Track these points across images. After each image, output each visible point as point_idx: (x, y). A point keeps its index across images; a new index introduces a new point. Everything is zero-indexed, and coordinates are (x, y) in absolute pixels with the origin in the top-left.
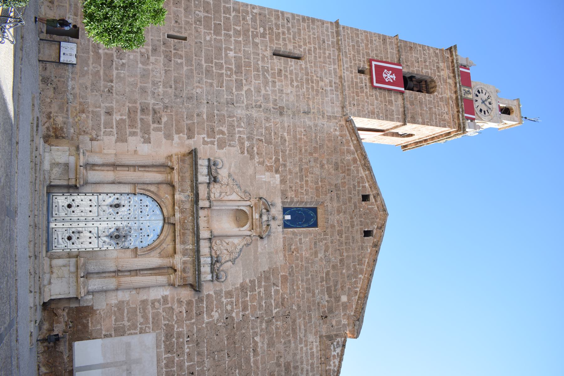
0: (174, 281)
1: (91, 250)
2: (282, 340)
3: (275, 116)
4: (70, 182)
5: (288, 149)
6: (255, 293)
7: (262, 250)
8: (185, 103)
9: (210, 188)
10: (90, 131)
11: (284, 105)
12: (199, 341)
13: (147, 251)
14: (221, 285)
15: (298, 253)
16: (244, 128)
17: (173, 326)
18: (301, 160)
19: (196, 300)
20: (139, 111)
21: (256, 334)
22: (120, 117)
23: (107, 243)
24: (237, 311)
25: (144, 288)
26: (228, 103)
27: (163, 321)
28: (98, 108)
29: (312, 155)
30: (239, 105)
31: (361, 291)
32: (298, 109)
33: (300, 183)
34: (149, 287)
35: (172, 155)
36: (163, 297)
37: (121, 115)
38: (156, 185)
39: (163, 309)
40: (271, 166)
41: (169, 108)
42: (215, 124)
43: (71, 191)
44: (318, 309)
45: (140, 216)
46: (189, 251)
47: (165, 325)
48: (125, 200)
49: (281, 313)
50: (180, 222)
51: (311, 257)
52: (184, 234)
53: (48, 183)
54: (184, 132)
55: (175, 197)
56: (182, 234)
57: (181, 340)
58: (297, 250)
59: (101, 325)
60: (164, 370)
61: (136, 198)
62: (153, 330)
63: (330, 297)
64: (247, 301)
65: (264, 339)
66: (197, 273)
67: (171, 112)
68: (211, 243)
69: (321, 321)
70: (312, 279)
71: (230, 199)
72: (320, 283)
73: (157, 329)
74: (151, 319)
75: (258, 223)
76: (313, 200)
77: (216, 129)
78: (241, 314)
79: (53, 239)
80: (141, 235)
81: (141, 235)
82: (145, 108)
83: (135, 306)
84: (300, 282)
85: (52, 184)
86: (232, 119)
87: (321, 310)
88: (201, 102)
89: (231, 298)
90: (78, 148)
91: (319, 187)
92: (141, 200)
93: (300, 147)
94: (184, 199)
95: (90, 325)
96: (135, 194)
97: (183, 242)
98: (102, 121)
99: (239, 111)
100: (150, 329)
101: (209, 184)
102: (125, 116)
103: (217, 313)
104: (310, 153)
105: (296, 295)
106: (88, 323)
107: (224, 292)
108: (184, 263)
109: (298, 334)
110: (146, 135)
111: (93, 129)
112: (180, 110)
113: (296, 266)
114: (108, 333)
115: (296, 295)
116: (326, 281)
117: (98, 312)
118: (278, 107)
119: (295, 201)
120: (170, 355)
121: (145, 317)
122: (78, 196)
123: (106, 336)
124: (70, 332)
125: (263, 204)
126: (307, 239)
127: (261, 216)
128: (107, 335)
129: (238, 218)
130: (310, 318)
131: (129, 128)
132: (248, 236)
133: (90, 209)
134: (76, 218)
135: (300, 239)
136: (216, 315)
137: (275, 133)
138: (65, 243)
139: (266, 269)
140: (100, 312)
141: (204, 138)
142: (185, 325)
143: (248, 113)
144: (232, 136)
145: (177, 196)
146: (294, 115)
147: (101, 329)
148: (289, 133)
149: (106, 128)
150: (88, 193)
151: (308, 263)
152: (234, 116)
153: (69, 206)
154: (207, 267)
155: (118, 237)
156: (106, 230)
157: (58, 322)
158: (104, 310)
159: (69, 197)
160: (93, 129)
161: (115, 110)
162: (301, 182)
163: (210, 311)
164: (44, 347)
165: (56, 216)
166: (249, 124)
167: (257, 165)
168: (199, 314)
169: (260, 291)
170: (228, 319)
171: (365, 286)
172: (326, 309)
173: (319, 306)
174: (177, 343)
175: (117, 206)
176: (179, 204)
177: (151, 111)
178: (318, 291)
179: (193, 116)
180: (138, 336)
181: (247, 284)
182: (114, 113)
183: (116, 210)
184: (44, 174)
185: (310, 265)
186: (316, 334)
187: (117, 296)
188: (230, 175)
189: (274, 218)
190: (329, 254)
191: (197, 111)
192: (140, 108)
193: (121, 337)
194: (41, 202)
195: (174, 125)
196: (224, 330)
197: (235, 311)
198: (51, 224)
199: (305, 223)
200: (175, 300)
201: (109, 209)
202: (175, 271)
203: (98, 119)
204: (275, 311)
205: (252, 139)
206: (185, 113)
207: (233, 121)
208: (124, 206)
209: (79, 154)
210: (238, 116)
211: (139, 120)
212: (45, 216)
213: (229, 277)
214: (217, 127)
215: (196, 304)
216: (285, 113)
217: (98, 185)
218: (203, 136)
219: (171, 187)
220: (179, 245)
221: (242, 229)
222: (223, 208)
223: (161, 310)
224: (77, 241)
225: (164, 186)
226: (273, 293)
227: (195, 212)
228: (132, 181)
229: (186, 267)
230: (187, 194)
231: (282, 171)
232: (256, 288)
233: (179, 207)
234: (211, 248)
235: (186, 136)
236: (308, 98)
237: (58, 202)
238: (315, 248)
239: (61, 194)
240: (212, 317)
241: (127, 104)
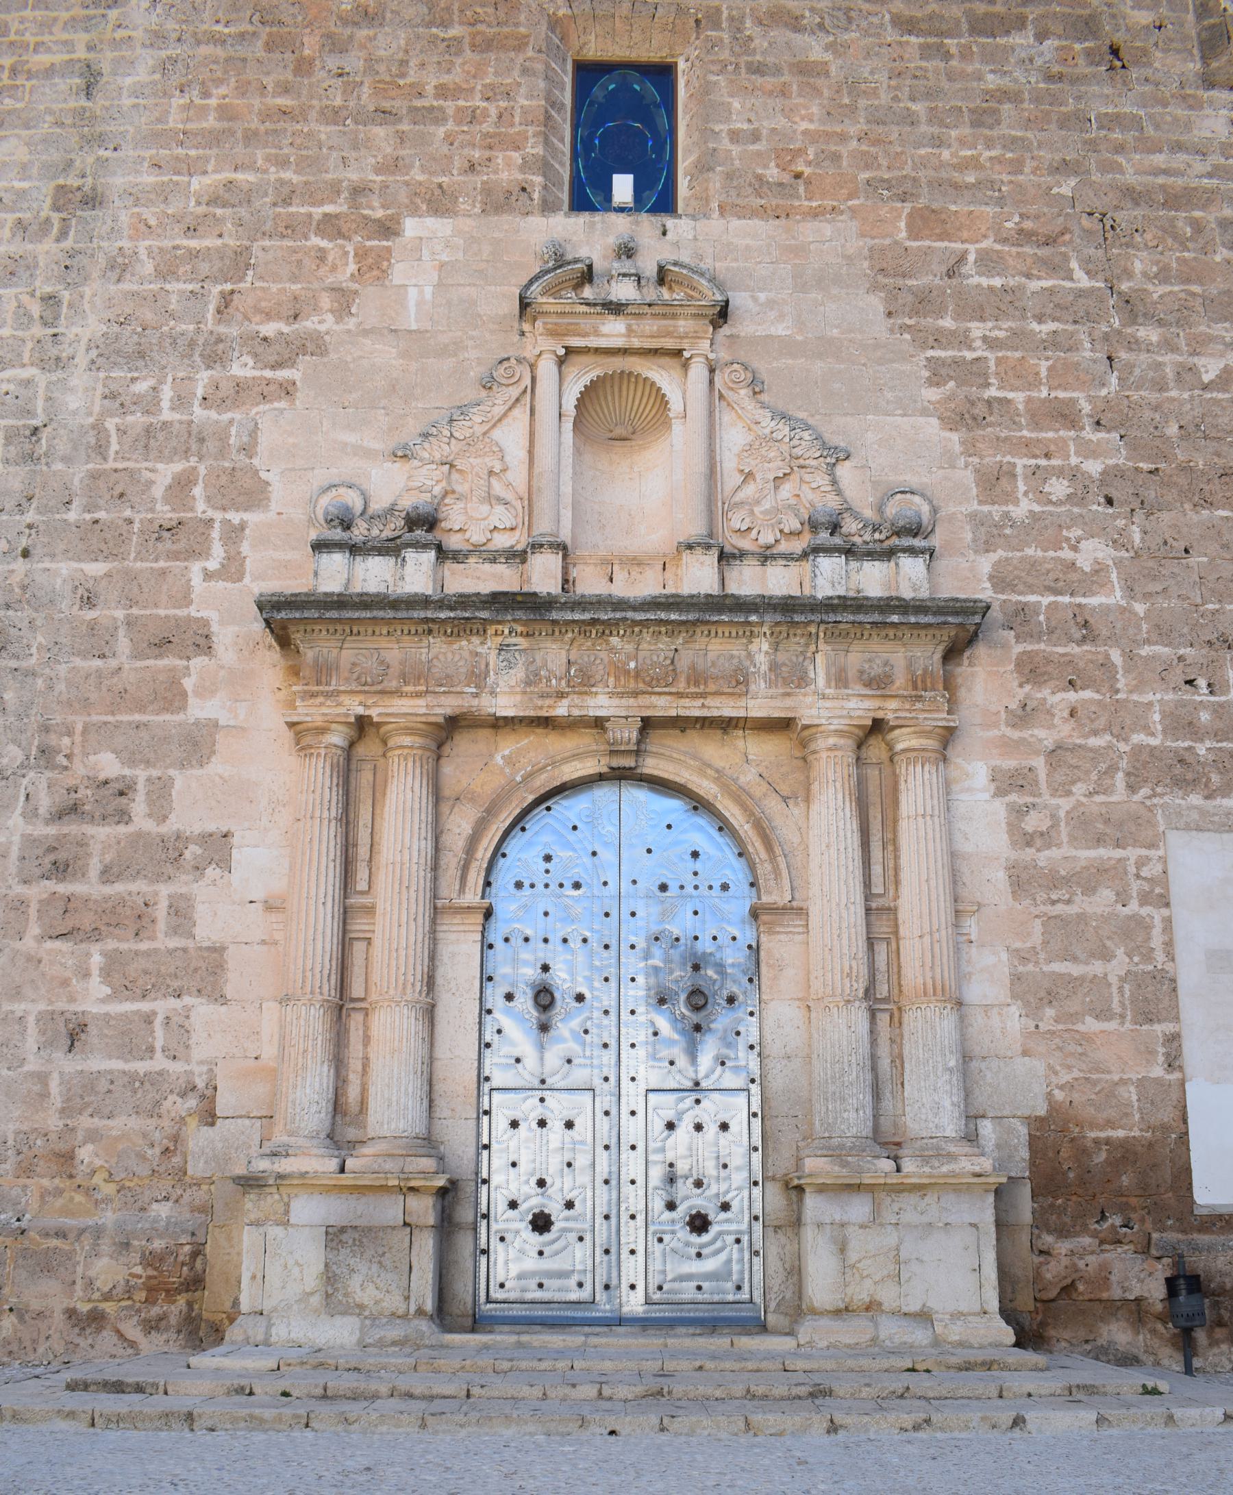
0: (923, 733)
1: (757, 1123)
2: (1218, 258)
3: (106, 228)
4: (422, 1222)
5: (273, 174)
6: (992, 364)
7: (781, 317)
8: (24, 664)
9: (465, 547)
10: (166, 1123)
11: (48, 188)
12: (1213, 637)
13: (773, 858)
14: (951, 518)
15: (801, 152)
16: (161, 382)
17: (1138, 749)
18: (333, 116)
19: (1017, 637)
20: (63, 888)
21: (1186, 374)
22: (96, 979)
23: (725, 1051)
24: (1077, 453)
25: (955, 878)
26: (30, 457)
27: (1114, 799)
28: (46, 1085)
29: (311, 62)
30: (40, 404)
32: (69, 121)
33: (450, 125)
34: (953, 855)
35: (291, 725)
36: (1000, 793)
37: (87, 975)
38: (445, 808)
39: (1054, 793)
40: (361, 255)
41: (53, 739)
42: (137, 518)
43: (465, 1214)
44: (1076, 80)
45: (598, 890)
46: (781, 657)
47: (1132, 788)
48: (515, 962)
49: (1092, 251)
50: (635, 694)
51: (826, 93)
52: (696, 677)
53: (424, 1325)
54: (172, 669)
55: (510, 713)
56: (697, 684)
57: (1205, 716)
58: (787, 156)
59: (1123, 1082)
61: (507, 905)
62: (1152, 846)
63: (1020, 23)
64: (1029, 400)
65: (1211, 339)
66: (895, 618)
67: (70, 733)
68: (741, 555)
69: (1134, 73)
70: (929, 95)
71: (523, 454)
72: (954, 63)
73: (1152, 824)
74: (1102, 852)
75: (650, 325)
76: (539, 67)
77: (165, 513)
78: (1089, 434)
79: (700, 1297)
80: (689, 889)
81: (689, 889)
82: (52, 857)
83: (1038, 922)
84: (946, 154)
85: (429, 1306)
86: (114, 439)
87: (1083, 67)
88: (24, 588)
89: (1014, 476)
90: (250, 1183)
91: (473, 36)
92: (519, 885)
93: (265, 116)
94: (519, 673)
95: (1121, 1133)
96: (488, 913)
97: (740, 682)
98: (117, 1065)
99: (74, 402)
100: (1148, 859)
101: (442, 553)
102: (88, 955)
103: (1084, 545)
104: (298, 71)
105: (1005, 177)
106: (1108, 1141)
107: (986, 508)
108: (840, 679)
109: (1194, 183)
110: (188, 854)
111: (154, 1111)
112: (61, 687)
113: (867, 167)
114: (1161, 1050)
115: (1005, 177)
116: (942, 34)
117: (1059, 1095)
118: (56, 217)
119: (539, 150)
121: (1091, 878)
122: (493, 1183)
123: (1173, 1062)
124: (1149, 1226)
125: (553, 291)
126: (736, 105)
127: (615, 308)
128: (1167, 1055)
129: (619, 431)
130: (1114, 121)
131: (152, 938)
132: (711, 382)
133: (556, 1125)
134: (601, 1189)
135: (735, 136)
136: (1092, 552)
137: (191, 230)
138: (718, 1244)
139: (876, 304)
140: (1061, 1088)
141: (208, 576)
142: (1135, 697)
143: (82, 360)
144: (202, 440)
145: (505, 706)
146: (100, 140)
147: (1141, 1083)
148: (192, 168)
149: (151, 1050)
150: (479, 1135)
151: (853, 109)
152: (99, 428)
153: (541, 1223)
154: (861, 576)
155: (698, 999)
156: (665, 1053)
157: (1103, 1278)
158: (1050, 1067)
159: (494, 1227)
160: (154, 1111)
161: (61, 1005)
162: (445, 120)
163: (1074, 576)
164: (1214, 1343)
165: (588, 1286)
166: (142, 355)
167: (351, 323)
168: (1086, 629)
169: (985, 339)
170: (1114, 494)
172: (1077, 47)
173: (1060, 77)
174: (1218, 735)
175: (544, 998)
176: (542, 696)
177: (65, 830)
178: (990, 77)
179: (92, 626)
180: (1179, 912)
181: (950, 398)
182: (73, 1007)
183: (563, 1002)
184: (381, 1344)
185: (862, 103)
186: (1195, 105)
187: (987, 1008)
188: (403, 455)
189: (627, 251)
190: (812, 10)
191: (67, 606)
192: (51, 885)
193: (1181, 992)
194: (524, 1365)
195: (137, 717)
196: (1166, 517)
197: (1074, 460)
198: (625, 1309)
199: (649, 121)
200: (1016, 734)
201: (562, 1040)
202: (877, 727)
203: (103, 1085)
204: (1083, 281)
205: (220, 340)
206: (78, 662)
207: (122, 432)
208: (545, 968)
209: (280, 1176)
210: (97, 409)
211: (108, 890)
212: (594, 1340)
213: (913, 480)
214: (152, 510)
215: (1039, 640)
216: (90, 180)
217: (439, 1087)
218: (196, 579)
219: (457, 737)
220: (751, 703)
221: (676, 405)
222: (567, 489)
223: (1061, 801)
224: (714, 1189)
225: (447, 769)
226: (997, 282)
227: (587, 616)
228: (424, 921)
229: (862, 672)
230: (494, 653)
231: (383, 206)
232: (969, 355)
233: (561, 695)
234: (766, 556)
235: (198, 662)
236: (14, 71)
237: (520, 1277)
238: (778, 71)
239: (483, 1259)
240: (1099, 570)
241: (29, 943)
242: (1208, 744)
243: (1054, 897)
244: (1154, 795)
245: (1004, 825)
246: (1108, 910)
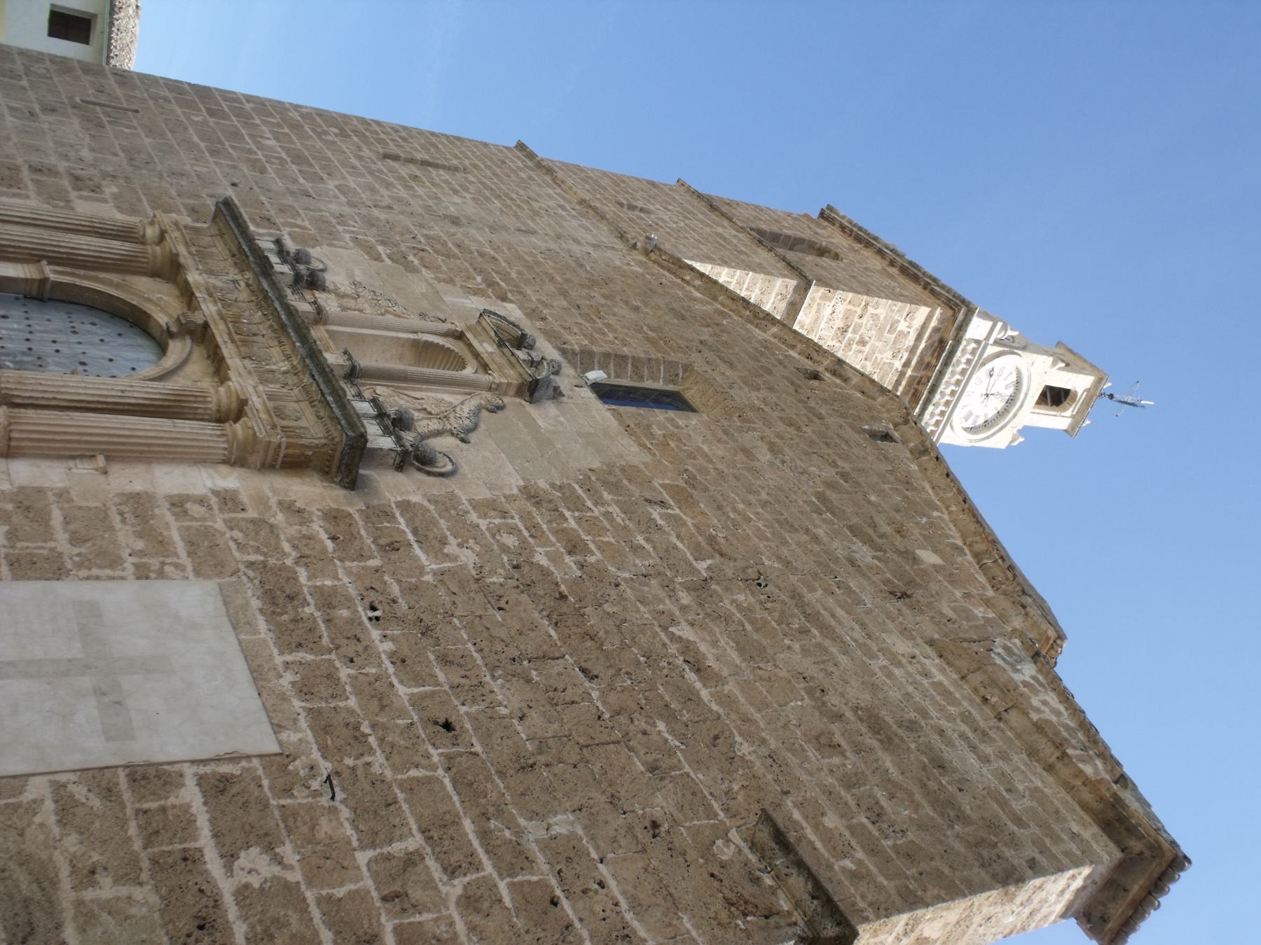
31: (969, 540)
47: (251, 565)
60: (297, 704)
120: (310, 657)
171: (972, 527)
242: (317, 614)
246: (123, 544)
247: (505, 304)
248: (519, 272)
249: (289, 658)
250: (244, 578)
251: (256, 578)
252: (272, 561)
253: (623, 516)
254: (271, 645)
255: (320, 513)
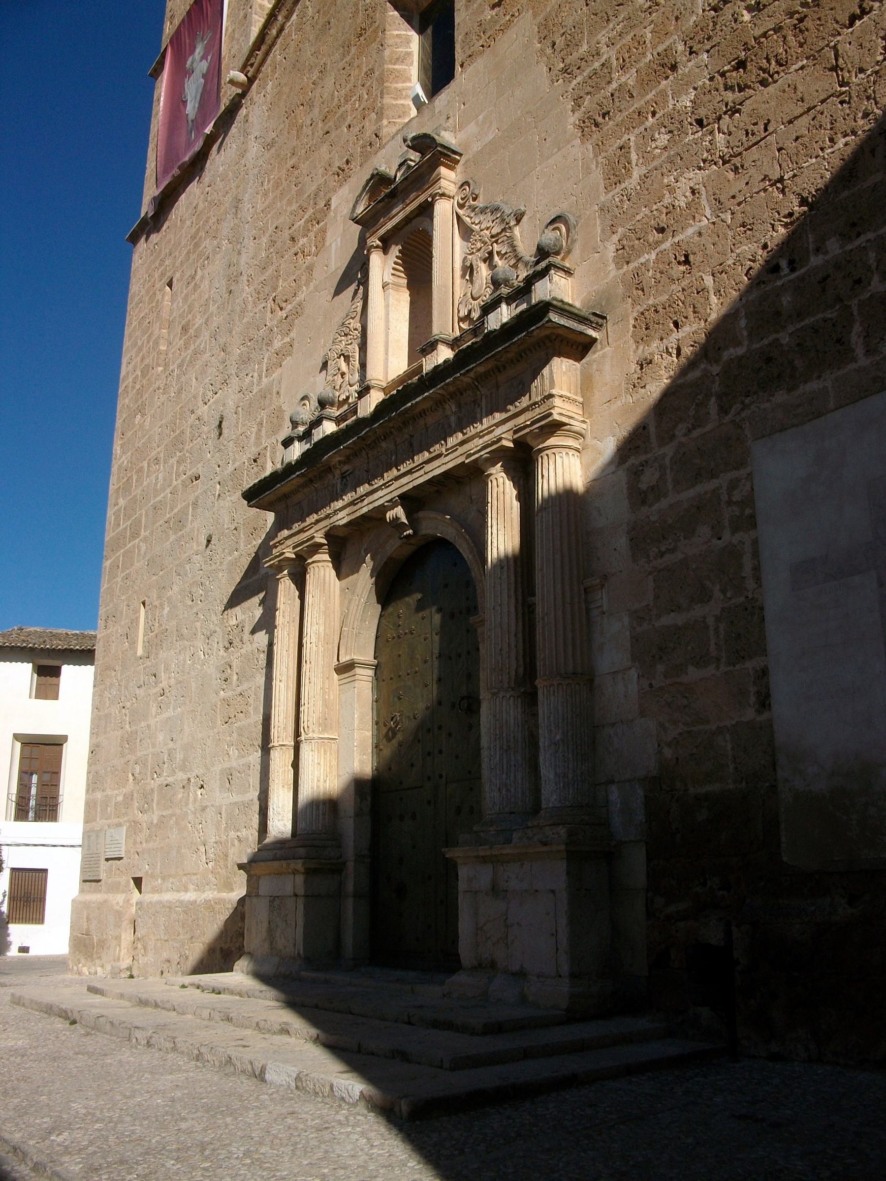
47: (723, 410)
74: (700, 489)
117: (668, 753)
120: (857, 328)
123: (764, 702)
128: (758, 693)
242: (791, 329)
243: (663, 549)
244: (745, 407)
245: (625, 491)
247: (333, 208)
248: (290, 203)
249: (860, 351)
250: (743, 415)
251: (742, 403)
252: (716, 387)
253: (611, 26)
254: (840, 373)
255: (641, 348)
